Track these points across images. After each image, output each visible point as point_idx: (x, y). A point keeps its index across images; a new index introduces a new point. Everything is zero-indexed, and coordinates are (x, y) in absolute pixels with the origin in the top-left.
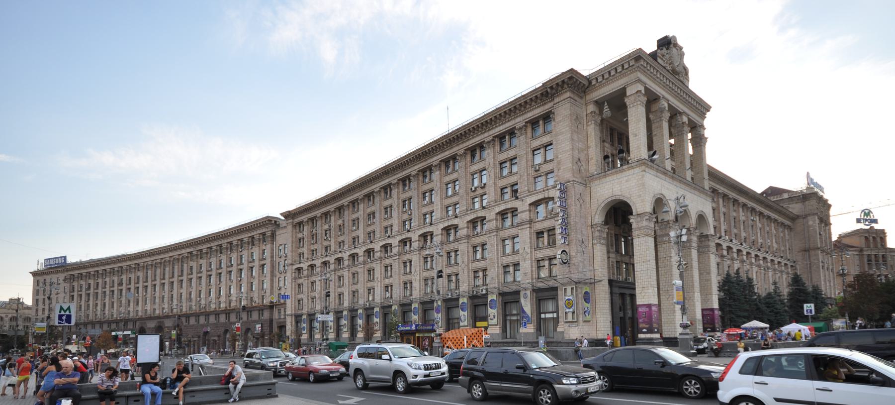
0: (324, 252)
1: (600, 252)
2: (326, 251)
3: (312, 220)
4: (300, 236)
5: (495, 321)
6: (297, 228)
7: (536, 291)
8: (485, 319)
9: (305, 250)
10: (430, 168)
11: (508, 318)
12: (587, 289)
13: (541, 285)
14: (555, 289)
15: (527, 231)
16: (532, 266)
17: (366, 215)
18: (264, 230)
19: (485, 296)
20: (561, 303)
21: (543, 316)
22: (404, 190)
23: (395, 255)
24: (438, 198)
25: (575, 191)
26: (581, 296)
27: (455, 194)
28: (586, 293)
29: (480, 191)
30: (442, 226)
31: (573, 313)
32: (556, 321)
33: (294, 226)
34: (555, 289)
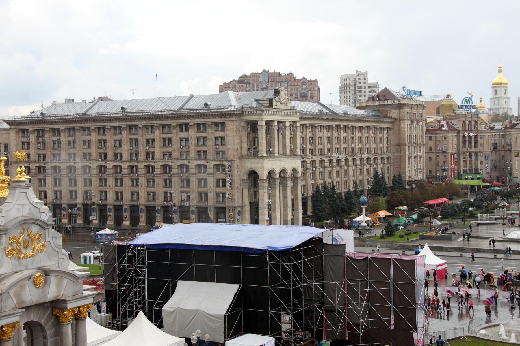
1: (246, 192)
6: (20, 133)
12: (239, 209)
17: (97, 140)
22: (130, 133)
25: (237, 163)
28: (239, 211)
30: (161, 164)
33: (17, 132)
34: (225, 208)
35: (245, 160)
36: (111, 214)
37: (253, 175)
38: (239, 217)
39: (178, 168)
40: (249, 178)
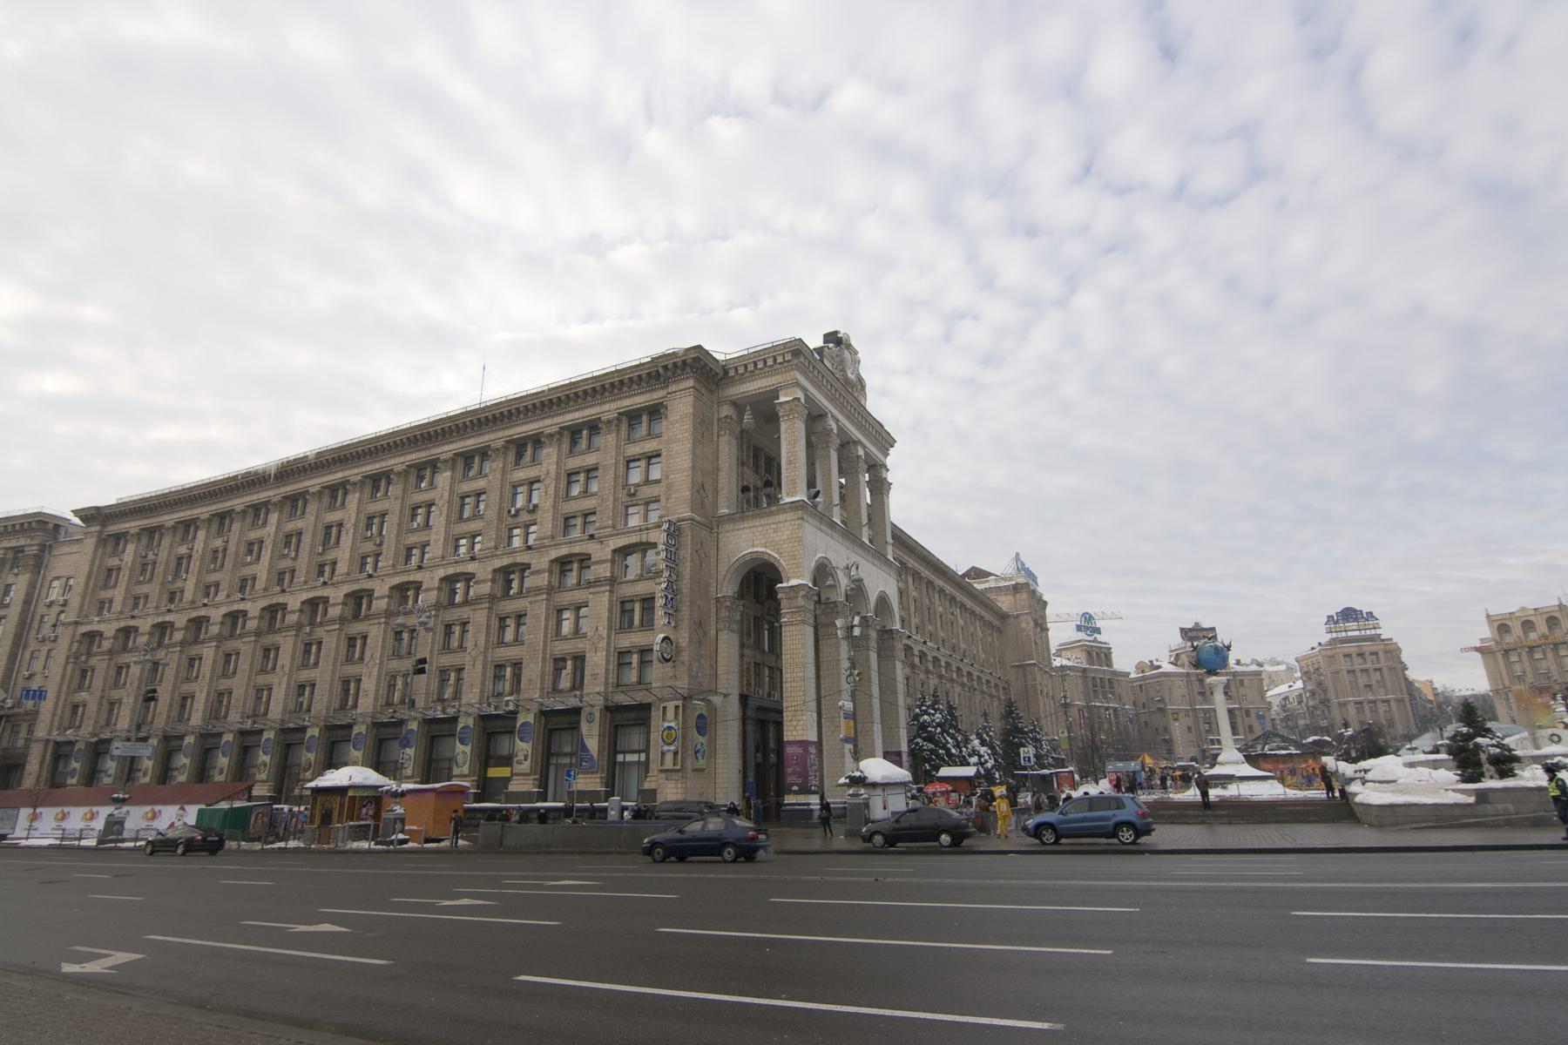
0: (164, 602)
2: (171, 600)
3: (151, 532)
4: (114, 562)
5: (525, 767)
7: (612, 710)
8: (507, 761)
9: (118, 594)
10: (434, 465)
11: (553, 760)
13: (622, 699)
14: (646, 708)
15: (605, 598)
16: (608, 661)
17: (281, 536)
18: (22, 542)
19: (512, 715)
20: (655, 736)
21: (620, 758)
22: (373, 496)
23: (333, 621)
24: (443, 520)
26: (692, 722)
27: (476, 516)
29: (524, 517)
30: (441, 573)
31: (676, 753)
32: (645, 766)
33: (102, 541)
34: (646, 708)
35: (730, 526)
36: (267, 759)
37: (760, 581)
38: (701, 739)
39: (493, 581)
40: (741, 595)
